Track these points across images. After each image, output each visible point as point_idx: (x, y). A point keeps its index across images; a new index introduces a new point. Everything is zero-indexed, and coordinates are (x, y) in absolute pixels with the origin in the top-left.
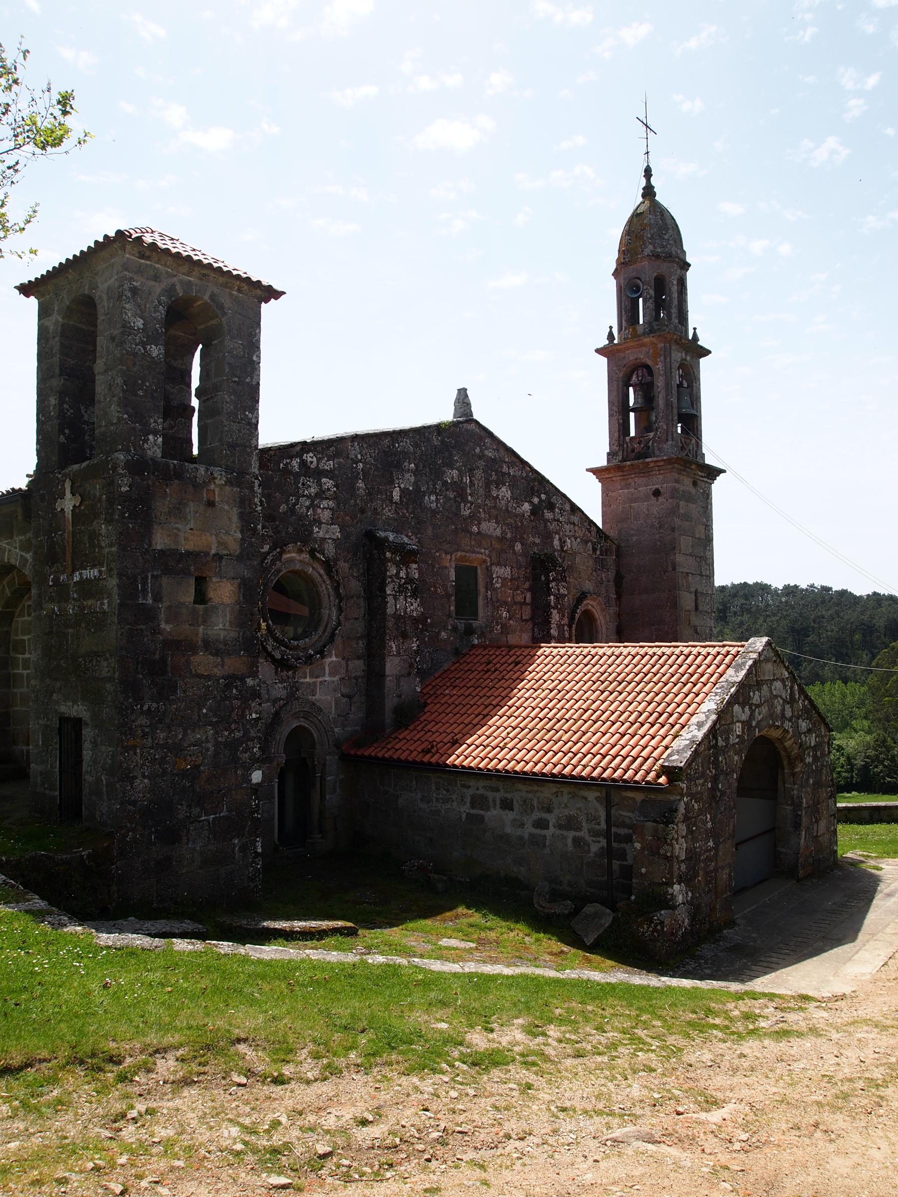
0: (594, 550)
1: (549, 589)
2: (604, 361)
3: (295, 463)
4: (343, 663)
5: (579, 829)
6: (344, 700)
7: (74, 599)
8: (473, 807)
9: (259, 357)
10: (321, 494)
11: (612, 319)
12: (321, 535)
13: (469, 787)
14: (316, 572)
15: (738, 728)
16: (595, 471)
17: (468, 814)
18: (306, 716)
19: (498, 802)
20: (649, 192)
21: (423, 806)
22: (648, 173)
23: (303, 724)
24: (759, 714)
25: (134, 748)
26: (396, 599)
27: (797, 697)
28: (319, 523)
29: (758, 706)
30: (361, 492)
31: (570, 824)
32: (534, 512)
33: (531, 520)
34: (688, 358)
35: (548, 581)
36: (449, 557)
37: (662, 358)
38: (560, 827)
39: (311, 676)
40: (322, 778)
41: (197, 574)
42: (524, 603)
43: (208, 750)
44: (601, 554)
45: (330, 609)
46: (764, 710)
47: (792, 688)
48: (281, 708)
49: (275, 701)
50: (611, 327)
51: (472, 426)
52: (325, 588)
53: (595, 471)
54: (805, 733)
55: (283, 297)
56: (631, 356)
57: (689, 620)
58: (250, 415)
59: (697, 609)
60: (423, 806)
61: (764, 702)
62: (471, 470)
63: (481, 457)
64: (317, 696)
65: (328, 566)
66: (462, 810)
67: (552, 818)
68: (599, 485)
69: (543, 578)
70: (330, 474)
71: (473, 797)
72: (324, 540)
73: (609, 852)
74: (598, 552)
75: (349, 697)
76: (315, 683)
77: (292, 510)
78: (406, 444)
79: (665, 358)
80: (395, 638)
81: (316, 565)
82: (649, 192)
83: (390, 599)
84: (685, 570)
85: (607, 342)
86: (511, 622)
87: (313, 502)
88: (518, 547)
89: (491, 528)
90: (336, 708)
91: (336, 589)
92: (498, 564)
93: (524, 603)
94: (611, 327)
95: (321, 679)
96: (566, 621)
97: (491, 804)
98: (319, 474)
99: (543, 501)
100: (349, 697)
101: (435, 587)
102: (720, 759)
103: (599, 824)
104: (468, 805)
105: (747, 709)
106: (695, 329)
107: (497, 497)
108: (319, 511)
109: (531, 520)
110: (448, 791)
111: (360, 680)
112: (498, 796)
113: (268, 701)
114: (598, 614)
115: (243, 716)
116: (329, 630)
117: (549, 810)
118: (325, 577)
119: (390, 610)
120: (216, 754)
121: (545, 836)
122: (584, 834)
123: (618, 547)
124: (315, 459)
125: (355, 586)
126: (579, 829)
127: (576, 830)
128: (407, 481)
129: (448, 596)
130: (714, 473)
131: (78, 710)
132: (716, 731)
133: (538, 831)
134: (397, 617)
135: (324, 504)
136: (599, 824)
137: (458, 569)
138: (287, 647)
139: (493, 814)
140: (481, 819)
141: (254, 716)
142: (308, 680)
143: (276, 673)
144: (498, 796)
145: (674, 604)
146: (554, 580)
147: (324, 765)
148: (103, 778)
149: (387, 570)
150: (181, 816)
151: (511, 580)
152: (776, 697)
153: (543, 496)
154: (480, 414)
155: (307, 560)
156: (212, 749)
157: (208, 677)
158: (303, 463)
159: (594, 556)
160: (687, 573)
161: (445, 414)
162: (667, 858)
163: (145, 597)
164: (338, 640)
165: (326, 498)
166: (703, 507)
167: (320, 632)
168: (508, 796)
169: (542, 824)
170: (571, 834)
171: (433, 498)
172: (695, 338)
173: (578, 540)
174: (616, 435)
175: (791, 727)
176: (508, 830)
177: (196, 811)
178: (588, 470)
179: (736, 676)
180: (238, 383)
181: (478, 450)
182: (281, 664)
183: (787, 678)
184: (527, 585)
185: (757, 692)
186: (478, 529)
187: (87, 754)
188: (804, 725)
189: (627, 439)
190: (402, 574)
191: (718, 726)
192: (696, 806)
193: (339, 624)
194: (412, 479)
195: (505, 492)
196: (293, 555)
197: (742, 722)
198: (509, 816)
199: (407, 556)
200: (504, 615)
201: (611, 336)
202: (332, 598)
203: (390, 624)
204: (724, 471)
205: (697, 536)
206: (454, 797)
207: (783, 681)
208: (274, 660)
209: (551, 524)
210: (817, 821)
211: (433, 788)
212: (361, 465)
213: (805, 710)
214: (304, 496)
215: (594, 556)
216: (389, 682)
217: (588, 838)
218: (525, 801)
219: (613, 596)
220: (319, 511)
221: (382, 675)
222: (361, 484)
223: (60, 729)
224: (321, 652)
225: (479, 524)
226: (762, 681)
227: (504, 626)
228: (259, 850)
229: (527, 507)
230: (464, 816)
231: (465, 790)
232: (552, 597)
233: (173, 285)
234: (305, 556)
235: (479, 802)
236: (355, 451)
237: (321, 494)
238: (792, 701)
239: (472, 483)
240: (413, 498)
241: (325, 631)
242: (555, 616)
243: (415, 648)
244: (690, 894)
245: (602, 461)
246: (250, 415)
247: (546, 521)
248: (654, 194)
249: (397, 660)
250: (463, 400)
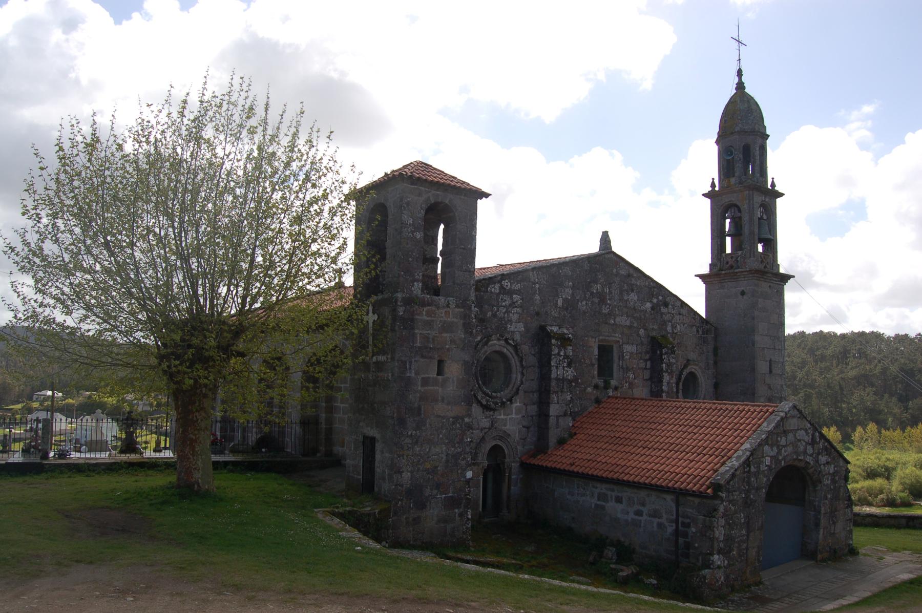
0: (698, 331)
1: (662, 360)
2: (708, 201)
3: (497, 286)
4: (524, 407)
5: (660, 517)
6: (524, 429)
7: (373, 371)
8: (599, 500)
9: (476, 232)
10: (513, 304)
11: (715, 174)
12: (512, 329)
13: (596, 488)
14: (508, 351)
15: (767, 461)
16: (701, 277)
17: (596, 505)
18: (501, 438)
19: (614, 497)
20: (740, 86)
21: (569, 497)
22: (740, 73)
23: (499, 443)
24: (785, 452)
25: (403, 455)
26: (557, 368)
27: (818, 440)
28: (510, 321)
29: (784, 446)
30: (538, 302)
31: (655, 514)
32: (653, 308)
33: (651, 314)
34: (767, 200)
35: (661, 354)
36: (594, 340)
37: (747, 201)
38: (650, 515)
39: (504, 415)
40: (510, 477)
41: (439, 359)
42: (646, 369)
43: (442, 458)
44: (703, 333)
45: (517, 374)
46: (790, 449)
47: (813, 435)
48: (485, 433)
49: (482, 430)
50: (713, 179)
51: (611, 255)
52: (514, 361)
53: (701, 277)
54: (824, 465)
55: (490, 197)
56: (726, 199)
57: (764, 380)
58: (470, 267)
59: (771, 372)
60: (569, 497)
61: (790, 444)
62: (610, 284)
63: (617, 274)
64: (508, 427)
65: (515, 347)
66: (592, 501)
67: (645, 510)
68: (704, 286)
69: (658, 352)
70: (518, 292)
71: (599, 494)
72: (513, 332)
73: (677, 532)
74: (701, 333)
75: (528, 428)
76: (506, 419)
77: (494, 315)
78: (567, 270)
79: (749, 202)
80: (556, 392)
81: (509, 347)
82: (740, 86)
83: (554, 369)
85: (710, 189)
86: (636, 381)
87: (507, 309)
88: (642, 332)
89: (623, 320)
90: (519, 434)
91: (521, 361)
92: (628, 343)
93: (646, 369)
94: (713, 179)
95: (510, 416)
96: (674, 380)
97: (609, 498)
98: (510, 293)
99: (661, 301)
100: (528, 428)
101: (584, 359)
102: (752, 479)
103: (673, 515)
104: (596, 498)
105: (775, 448)
106: (773, 179)
108: (511, 315)
109: (651, 314)
110: (584, 489)
111: (534, 418)
112: (614, 494)
113: (478, 429)
114: (699, 374)
115: (463, 439)
116: (516, 386)
117: (643, 505)
118: (514, 355)
119: (553, 375)
120: (447, 461)
121: (641, 521)
122: (663, 520)
123: (716, 329)
124: (509, 284)
125: (532, 360)
126: (660, 517)
127: (659, 518)
128: (567, 293)
129: (593, 365)
130: (786, 278)
131: (372, 432)
132: (750, 462)
133: (637, 517)
134: (557, 379)
135: (515, 310)
136: (673, 515)
137: (600, 347)
138: (490, 397)
139: (611, 506)
140: (603, 508)
141: (468, 440)
142: (502, 417)
143: (483, 412)
144: (614, 494)
145: (753, 369)
146: (666, 353)
147: (511, 468)
148: (386, 470)
149: (551, 351)
150: (427, 495)
151: (636, 354)
152: (799, 440)
153: (660, 298)
154: (616, 248)
155: (503, 345)
156: (445, 457)
157: (443, 417)
158: (502, 287)
159: (697, 335)
160: (764, 348)
161: (594, 248)
162: (710, 538)
163: (410, 373)
164: (521, 393)
165: (516, 307)
166: (777, 302)
167: (510, 388)
168: (619, 494)
169: (639, 513)
170: (656, 520)
171: (584, 303)
172: (773, 185)
173: (686, 325)
174: (716, 252)
175: (812, 460)
176: (619, 515)
177: (435, 492)
178: (696, 276)
179: (767, 426)
180: (464, 249)
181: (615, 271)
182: (486, 408)
183: (810, 428)
184: (647, 357)
185: (783, 438)
186: (615, 321)
187: (378, 457)
188: (823, 459)
189: (724, 255)
190: (562, 353)
191: (751, 458)
192: (733, 508)
193: (522, 383)
194: (570, 292)
195: (633, 297)
196: (495, 342)
197: (771, 457)
198: (620, 507)
199: (564, 341)
200: (631, 376)
201: (713, 185)
202: (518, 367)
203: (553, 384)
204: (794, 277)
205: (772, 322)
206: (588, 493)
207: (806, 430)
208: (482, 405)
209: (666, 315)
210: (834, 523)
211: (576, 487)
212: (537, 286)
213: (826, 449)
214: (502, 306)
215: (697, 335)
216: (552, 420)
217: (667, 524)
218: (629, 498)
219: (711, 362)
220: (511, 315)
221: (547, 416)
222: (537, 297)
223: (363, 442)
224: (511, 400)
225: (615, 318)
226: (788, 430)
227: (631, 384)
228: (470, 517)
229: (648, 305)
230: (593, 506)
231: (594, 489)
232: (664, 365)
233: (429, 197)
234: (502, 342)
235: (602, 497)
236: (533, 277)
237: (513, 304)
238: (813, 443)
239: (610, 292)
240: (570, 305)
241: (513, 387)
242: (666, 377)
243: (569, 399)
244: (726, 562)
245: (706, 270)
246: (470, 267)
247: (662, 314)
248: (744, 88)
249: (557, 406)
250: (605, 239)
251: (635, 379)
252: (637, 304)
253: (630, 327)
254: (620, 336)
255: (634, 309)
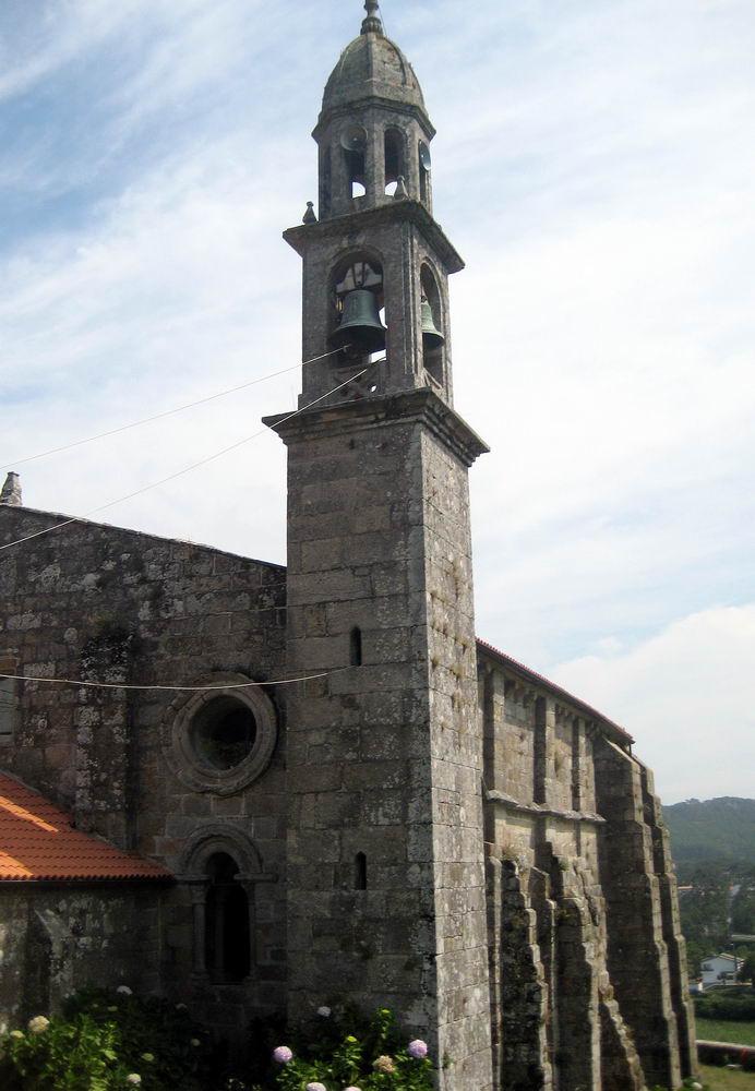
20: (370, 26)
59: (357, 658)
82: (370, 26)
84: (315, 599)
86: (53, 731)
107: (37, 581)
160: (323, 605)
195: (52, 571)
215: (257, 610)
251: (50, 726)
252: (59, 584)
253: (38, 631)
254: (16, 651)
255: (53, 594)
